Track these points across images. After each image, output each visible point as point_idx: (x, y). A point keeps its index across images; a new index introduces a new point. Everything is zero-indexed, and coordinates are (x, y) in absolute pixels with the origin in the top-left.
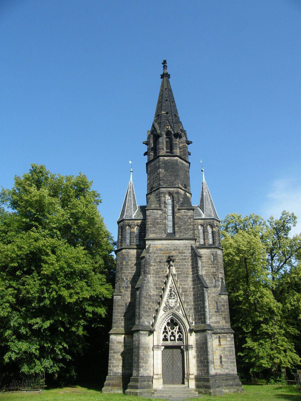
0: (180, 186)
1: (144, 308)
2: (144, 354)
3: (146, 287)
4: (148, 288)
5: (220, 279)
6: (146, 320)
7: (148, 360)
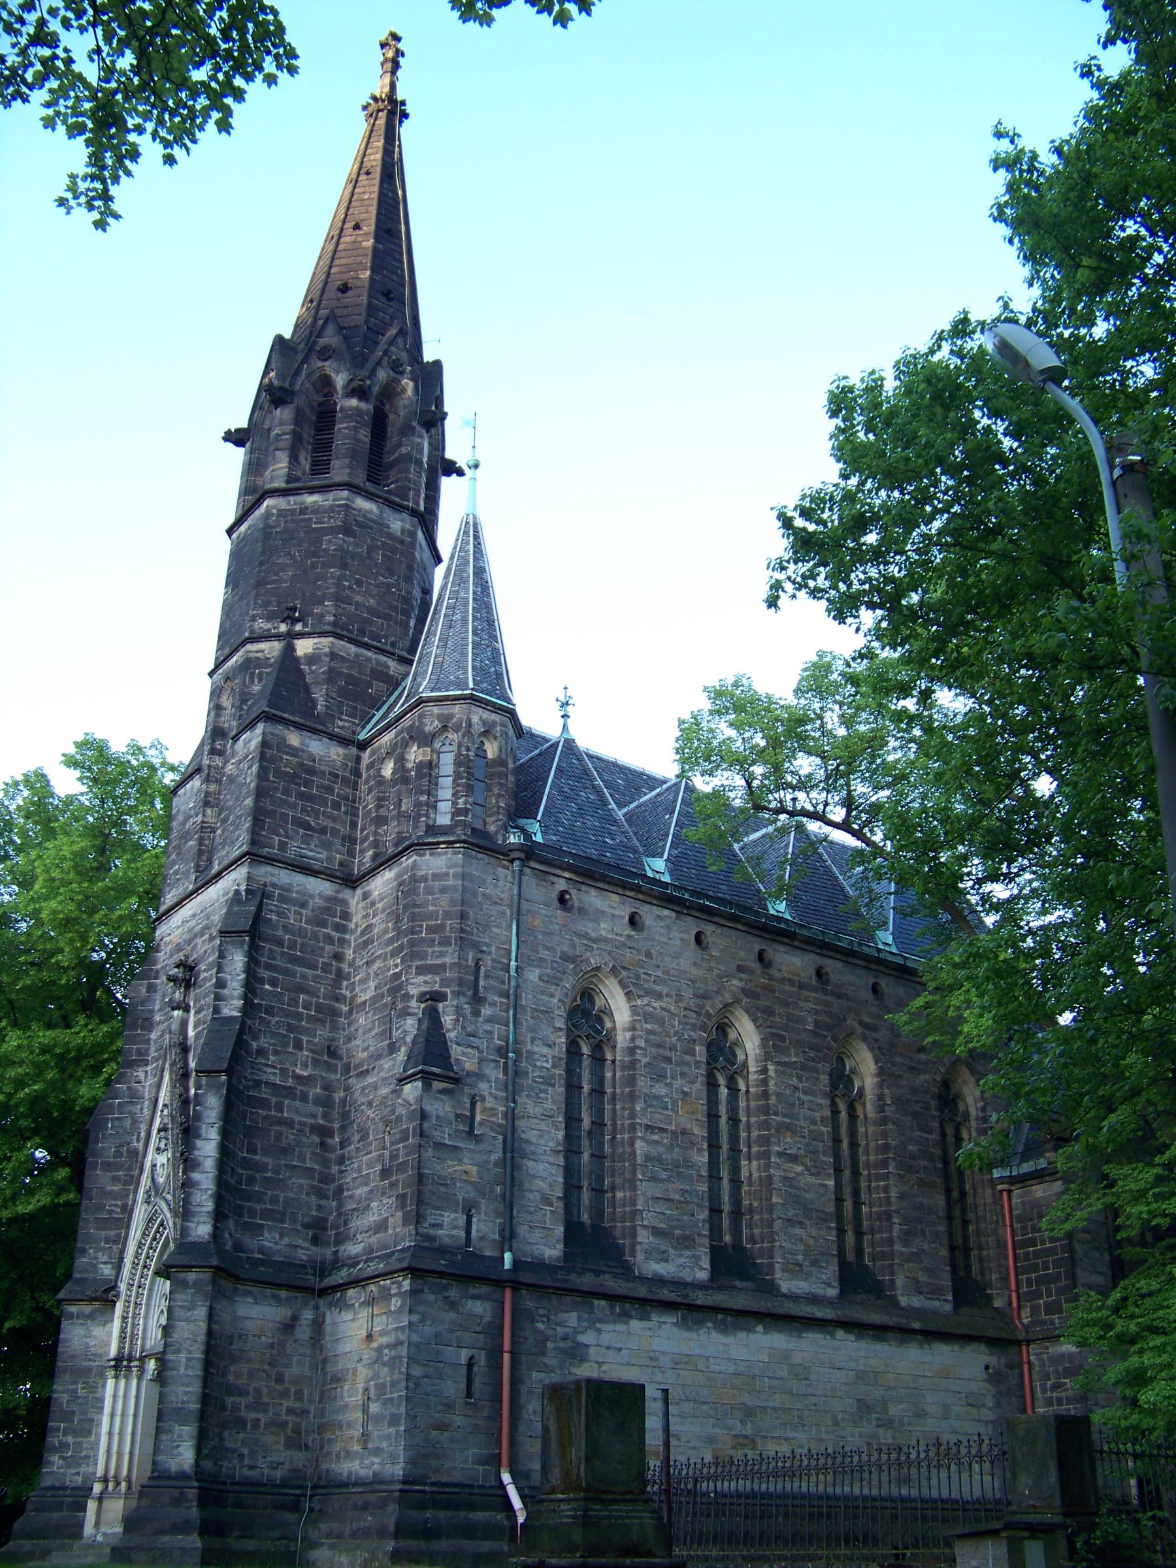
0: (261, 625)
1: (101, 1207)
2: (74, 1396)
3: (117, 1123)
4: (128, 1123)
5: (414, 1003)
6: (105, 1258)
7: (92, 1420)
